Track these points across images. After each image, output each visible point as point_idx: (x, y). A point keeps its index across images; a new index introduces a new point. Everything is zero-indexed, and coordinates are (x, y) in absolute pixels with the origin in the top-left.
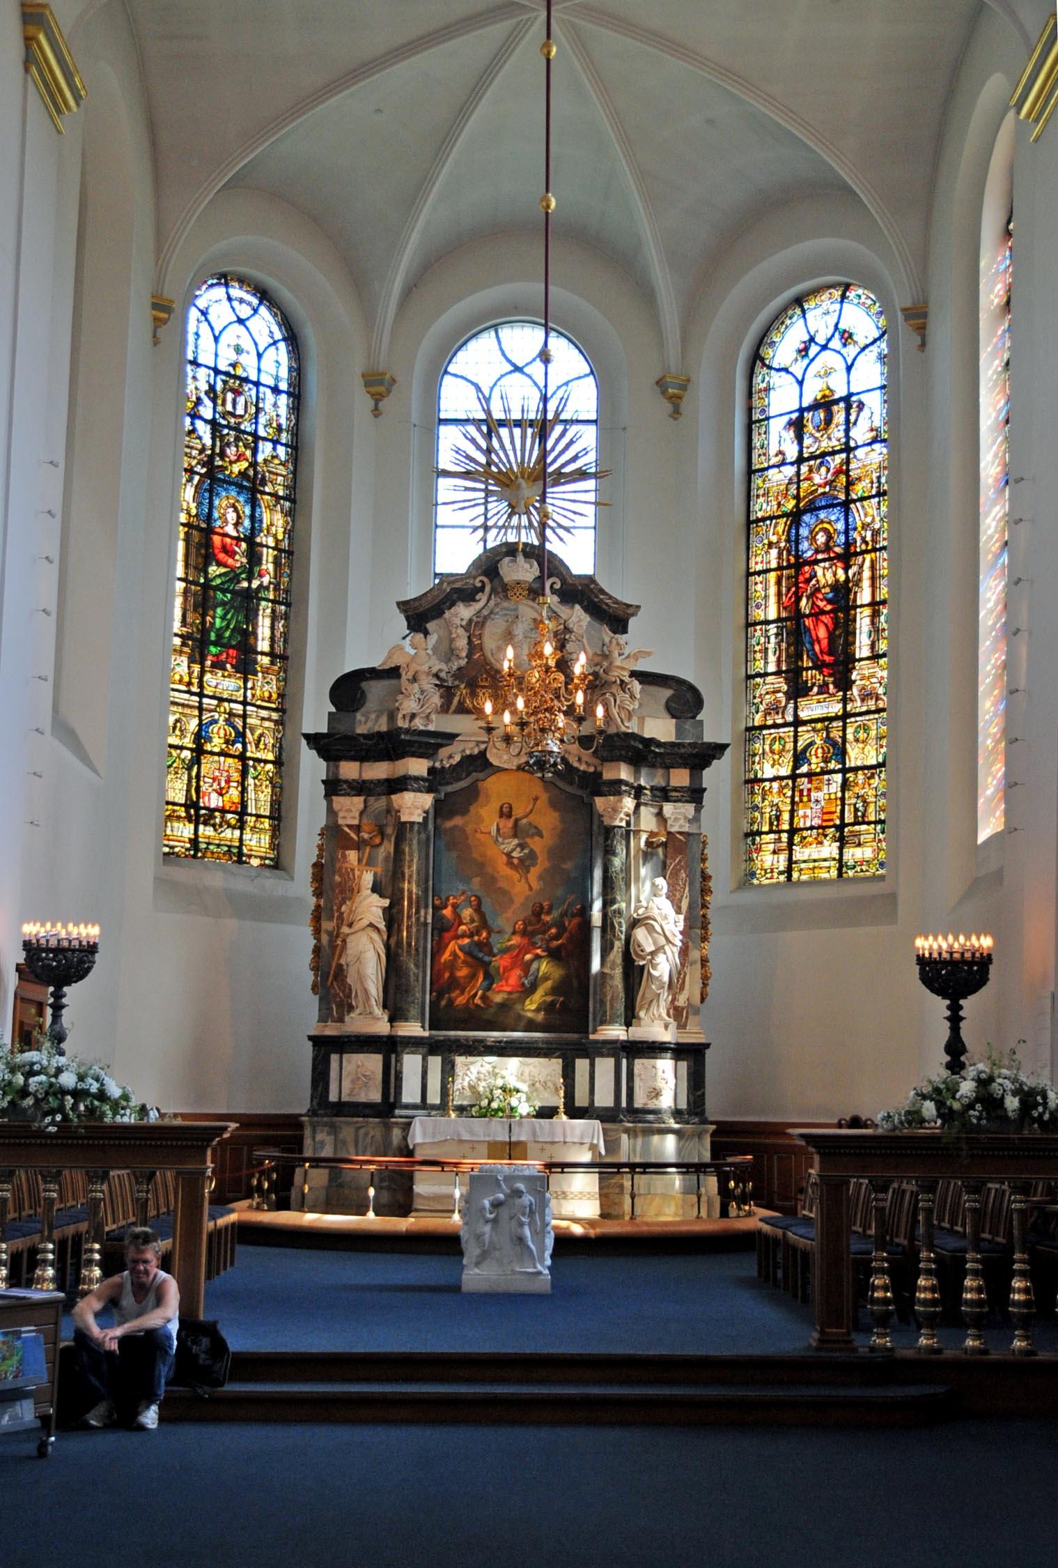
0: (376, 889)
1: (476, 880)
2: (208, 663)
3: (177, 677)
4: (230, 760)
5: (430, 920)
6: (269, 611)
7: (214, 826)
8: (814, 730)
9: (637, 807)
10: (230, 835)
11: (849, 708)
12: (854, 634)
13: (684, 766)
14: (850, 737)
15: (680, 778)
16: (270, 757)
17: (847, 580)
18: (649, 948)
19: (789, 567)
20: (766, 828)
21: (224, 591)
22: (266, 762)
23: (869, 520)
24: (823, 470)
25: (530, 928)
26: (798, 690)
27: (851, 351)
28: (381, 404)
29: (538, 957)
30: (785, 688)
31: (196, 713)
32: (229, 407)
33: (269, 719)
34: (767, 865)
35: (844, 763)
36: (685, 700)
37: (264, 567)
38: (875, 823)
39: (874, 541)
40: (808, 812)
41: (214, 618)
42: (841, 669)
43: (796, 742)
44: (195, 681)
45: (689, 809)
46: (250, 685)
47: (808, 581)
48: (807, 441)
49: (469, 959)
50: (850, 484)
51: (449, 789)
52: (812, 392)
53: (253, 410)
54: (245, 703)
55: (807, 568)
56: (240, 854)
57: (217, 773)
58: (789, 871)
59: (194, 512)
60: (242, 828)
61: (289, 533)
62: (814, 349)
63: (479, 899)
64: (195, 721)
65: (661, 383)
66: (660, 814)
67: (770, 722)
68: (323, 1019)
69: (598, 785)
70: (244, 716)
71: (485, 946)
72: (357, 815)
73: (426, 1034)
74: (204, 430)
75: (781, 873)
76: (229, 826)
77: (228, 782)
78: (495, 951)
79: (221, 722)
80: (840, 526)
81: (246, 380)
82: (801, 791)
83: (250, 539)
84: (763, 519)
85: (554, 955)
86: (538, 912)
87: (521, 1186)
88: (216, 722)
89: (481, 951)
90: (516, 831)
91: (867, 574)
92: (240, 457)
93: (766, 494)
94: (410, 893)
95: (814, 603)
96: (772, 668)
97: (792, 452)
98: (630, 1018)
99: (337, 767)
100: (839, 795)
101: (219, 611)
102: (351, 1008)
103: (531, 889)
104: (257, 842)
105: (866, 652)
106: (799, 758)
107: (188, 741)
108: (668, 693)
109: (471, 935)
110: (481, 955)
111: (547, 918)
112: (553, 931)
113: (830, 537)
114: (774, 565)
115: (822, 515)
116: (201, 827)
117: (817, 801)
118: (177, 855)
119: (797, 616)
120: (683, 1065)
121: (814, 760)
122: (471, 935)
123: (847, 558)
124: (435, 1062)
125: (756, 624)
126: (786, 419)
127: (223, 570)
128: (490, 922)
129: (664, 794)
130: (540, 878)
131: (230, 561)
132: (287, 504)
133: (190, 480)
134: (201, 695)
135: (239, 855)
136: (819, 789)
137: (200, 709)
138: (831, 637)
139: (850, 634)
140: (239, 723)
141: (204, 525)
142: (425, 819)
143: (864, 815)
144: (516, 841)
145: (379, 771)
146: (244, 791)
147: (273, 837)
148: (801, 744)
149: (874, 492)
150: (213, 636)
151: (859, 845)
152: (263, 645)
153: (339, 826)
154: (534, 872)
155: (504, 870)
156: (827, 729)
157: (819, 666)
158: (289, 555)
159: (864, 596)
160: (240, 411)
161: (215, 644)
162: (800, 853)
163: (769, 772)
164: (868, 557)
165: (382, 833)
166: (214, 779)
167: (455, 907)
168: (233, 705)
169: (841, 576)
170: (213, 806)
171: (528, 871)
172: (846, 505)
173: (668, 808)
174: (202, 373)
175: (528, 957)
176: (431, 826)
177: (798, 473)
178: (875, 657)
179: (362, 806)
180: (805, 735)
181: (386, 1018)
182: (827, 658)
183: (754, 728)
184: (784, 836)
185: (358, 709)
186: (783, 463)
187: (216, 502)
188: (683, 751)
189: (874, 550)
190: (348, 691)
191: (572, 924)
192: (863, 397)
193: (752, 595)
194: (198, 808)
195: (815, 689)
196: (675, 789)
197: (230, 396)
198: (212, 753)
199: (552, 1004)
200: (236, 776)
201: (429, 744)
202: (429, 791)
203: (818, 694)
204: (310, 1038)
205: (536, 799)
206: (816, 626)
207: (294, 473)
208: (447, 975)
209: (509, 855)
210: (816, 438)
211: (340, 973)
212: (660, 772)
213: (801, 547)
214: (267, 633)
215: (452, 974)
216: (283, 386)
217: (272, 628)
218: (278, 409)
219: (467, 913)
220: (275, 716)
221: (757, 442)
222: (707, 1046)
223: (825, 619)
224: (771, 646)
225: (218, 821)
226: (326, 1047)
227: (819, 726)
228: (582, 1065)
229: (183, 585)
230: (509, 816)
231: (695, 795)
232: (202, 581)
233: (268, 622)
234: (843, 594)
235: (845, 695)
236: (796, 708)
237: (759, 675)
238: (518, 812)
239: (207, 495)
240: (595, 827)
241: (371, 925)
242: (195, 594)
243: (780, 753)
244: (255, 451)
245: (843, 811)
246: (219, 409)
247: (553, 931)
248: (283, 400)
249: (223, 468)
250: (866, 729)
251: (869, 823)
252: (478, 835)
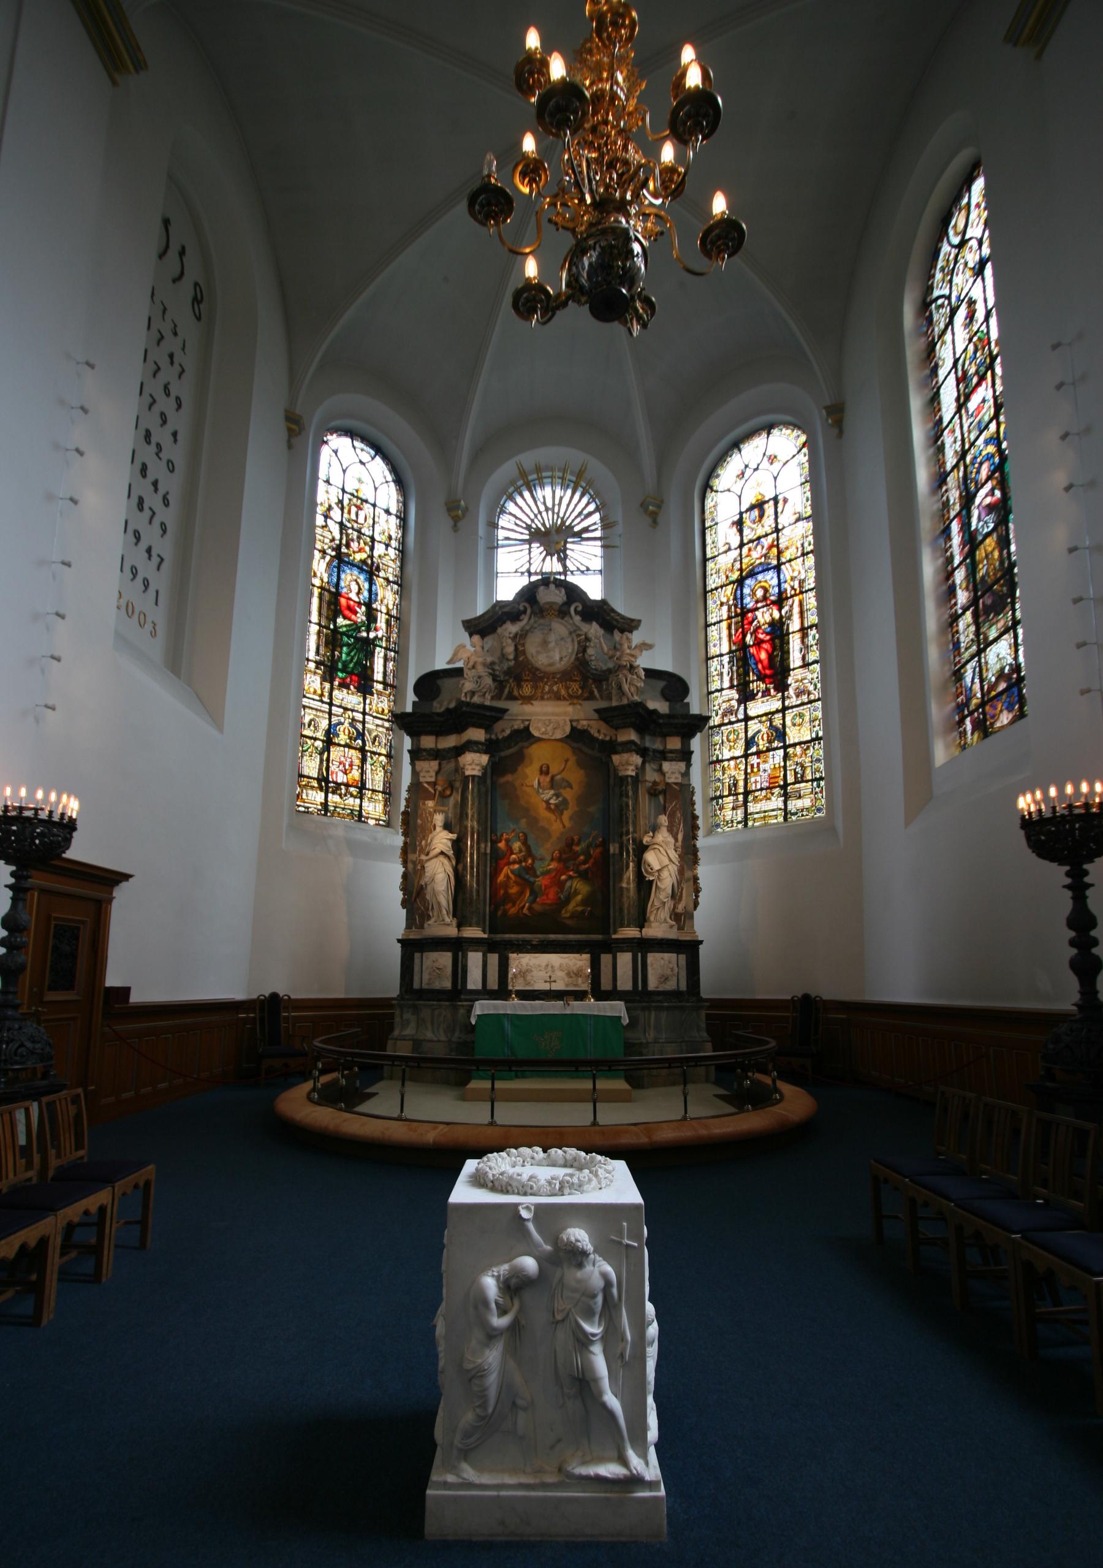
0: (447, 827)
1: (524, 821)
2: (336, 683)
3: (312, 690)
4: (352, 751)
5: (488, 851)
6: (382, 654)
7: (340, 795)
8: (760, 722)
9: (644, 763)
10: (352, 802)
11: (787, 703)
12: (788, 652)
13: (676, 734)
14: (788, 722)
15: (674, 743)
16: (384, 752)
17: (781, 617)
18: (656, 867)
19: (737, 615)
20: (726, 793)
21: (349, 637)
22: (380, 754)
23: (795, 574)
24: (759, 547)
25: (564, 856)
26: (746, 696)
27: (777, 465)
28: (459, 524)
29: (570, 877)
30: (737, 696)
31: (327, 716)
32: (353, 517)
33: (382, 726)
34: (728, 818)
35: (784, 742)
37: (378, 624)
38: (812, 781)
39: (801, 586)
40: (758, 778)
41: (341, 653)
43: (746, 732)
44: (326, 694)
45: (682, 766)
46: (368, 701)
47: (751, 623)
48: (746, 531)
49: (518, 880)
50: (780, 553)
51: (503, 754)
52: (749, 499)
53: (371, 522)
54: (364, 713)
55: (750, 615)
56: (360, 815)
57: (342, 759)
58: (745, 820)
59: (326, 580)
60: (361, 799)
61: (399, 606)
62: (748, 472)
63: (525, 835)
64: (327, 722)
65: (644, 505)
66: (660, 770)
67: (726, 721)
68: (409, 926)
69: (612, 747)
70: (364, 722)
71: (531, 870)
72: (434, 774)
73: (486, 936)
74: (335, 530)
75: (738, 823)
76: (352, 795)
77: (351, 765)
78: (538, 873)
79: (346, 725)
80: (775, 582)
81: (366, 501)
82: (752, 766)
83: (369, 605)
84: (716, 589)
85: (583, 876)
86: (570, 843)
87: (579, 1235)
88: (342, 724)
89: (527, 873)
90: (552, 784)
91: (796, 610)
92: (361, 550)
93: (718, 572)
94: (473, 828)
95: (756, 637)
96: (726, 684)
97: (735, 541)
98: (642, 921)
99: (419, 741)
100: (782, 764)
101: (345, 649)
102: (429, 918)
103: (564, 826)
105: (799, 663)
106: (749, 742)
107: (320, 735)
108: (661, 684)
109: (520, 862)
110: (527, 877)
111: (577, 848)
112: (582, 858)
113: (766, 590)
114: (725, 616)
115: (760, 577)
116: (330, 795)
117: (765, 771)
118: (311, 813)
119: (743, 647)
120: (683, 958)
121: (761, 742)
122: (520, 862)
123: (780, 602)
124: (494, 959)
125: (713, 657)
126: (730, 522)
127: (348, 622)
128: (534, 852)
129: (664, 755)
130: (571, 818)
131: (353, 617)
132: (396, 587)
133: (324, 558)
134: (331, 704)
135: (359, 816)
136: (765, 762)
137: (330, 714)
138: (770, 656)
139: (786, 653)
140: (360, 726)
141: (333, 590)
142: (484, 774)
143: (802, 776)
144: (552, 792)
145: (450, 741)
146: (363, 773)
147: (385, 805)
148: (750, 734)
149: (799, 554)
150: (340, 665)
151: (800, 797)
152: (378, 676)
153: (420, 783)
154: (566, 815)
155: (543, 813)
156: (770, 720)
157: (761, 678)
158: (397, 620)
159: (795, 625)
160: (361, 520)
161: (342, 671)
162: (752, 807)
163: (727, 754)
164: (796, 599)
165: (451, 786)
166: (340, 763)
167: (507, 841)
168: (355, 714)
169: (776, 615)
170: (339, 781)
171: (562, 814)
172: (778, 568)
173: (666, 766)
174: (332, 489)
175: (563, 877)
176: (489, 782)
177: (741, 555)
178: (806, 665)
179: (436, 768)
180: (753, 727)
181: (455, 922)
182: (768, 672)
183: (715, 727)
184: (741, 798)
185: (434, 699)
186: (729, 549)
187: (343, 576)
188: (676, 721)
189: (801, 593)
191: (595, 852)
192: (787, 495)
193: (710, 638)
194: (327, 781)
195: (760, 694)
196: (671, 751)
197: (354, 509)
198: (339, 745)
199: (583, 912)
200: (357, 762)
202: (485, 753)
203: (763, 696)
204: (399, 941)
205: (567, 761)
206: (759, 652)
207: (402, 567)
208: (502, 892)
209: (547, 802)
210: (753, 529)
211: (421, 890)
212: (659, 740)
213: (745, 601)
214: (381, 669)
215: (506, 892)
216: (393, 510)
217: (385, 666)
219: (516, 845)
220: (387, 724)
221: (709, 540)
222: (701, 942)
223: (765, 646)
224: (726, 670)
225: (343, 791)
226: (411, 947)
227: (764, 718)
228: (606, 959)
229: (317, 627)
230: (547, 773)
231: (686, 755)
232: (332, 627)
233: (381, 661)
235: (783, 695)
236: (746, 709)
237: (717, 691)
238: (554, 770)
239: (336, 570)
240: (612, 781)
241: (442, 853)
242: (327, 635)
243: (735, 741)
244: (372, 549)
245: (785, 775)
246: (346, 515)
247: (582, 858)
248: (393, 521)
249: (349, 555)
250: (801, 715)
251: (807, 781)
252: (525, 788)
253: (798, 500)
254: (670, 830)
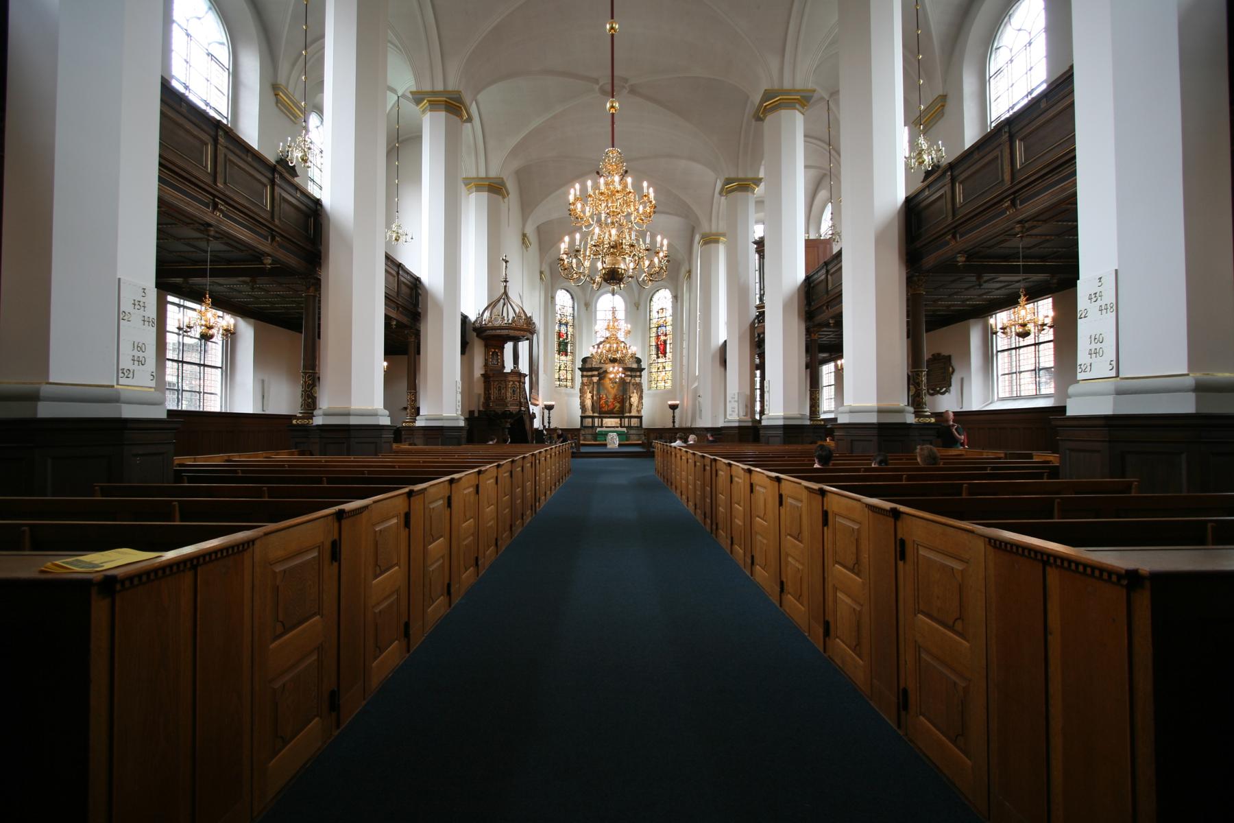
36: (639, 361)
42: (665, 353)
104: (569, 384)
190: (585, 360)
218: (570, 310)
226: (582, 418)
234: (665, 342)
253: (669, 311)
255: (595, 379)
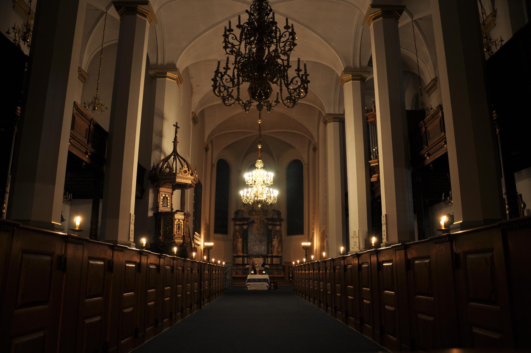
15: (278, 223)
98: (272, 253)
129: (276, 225)
201: (247, 219)
231: (280, 225)
254: (277, 238)
255: (245, 227)
